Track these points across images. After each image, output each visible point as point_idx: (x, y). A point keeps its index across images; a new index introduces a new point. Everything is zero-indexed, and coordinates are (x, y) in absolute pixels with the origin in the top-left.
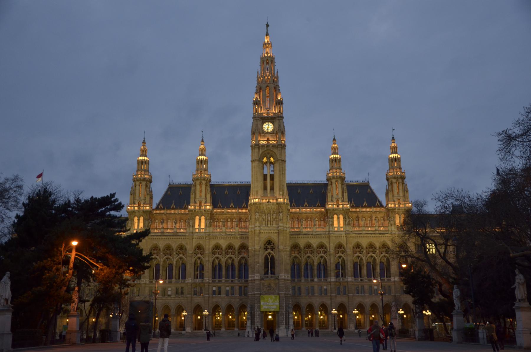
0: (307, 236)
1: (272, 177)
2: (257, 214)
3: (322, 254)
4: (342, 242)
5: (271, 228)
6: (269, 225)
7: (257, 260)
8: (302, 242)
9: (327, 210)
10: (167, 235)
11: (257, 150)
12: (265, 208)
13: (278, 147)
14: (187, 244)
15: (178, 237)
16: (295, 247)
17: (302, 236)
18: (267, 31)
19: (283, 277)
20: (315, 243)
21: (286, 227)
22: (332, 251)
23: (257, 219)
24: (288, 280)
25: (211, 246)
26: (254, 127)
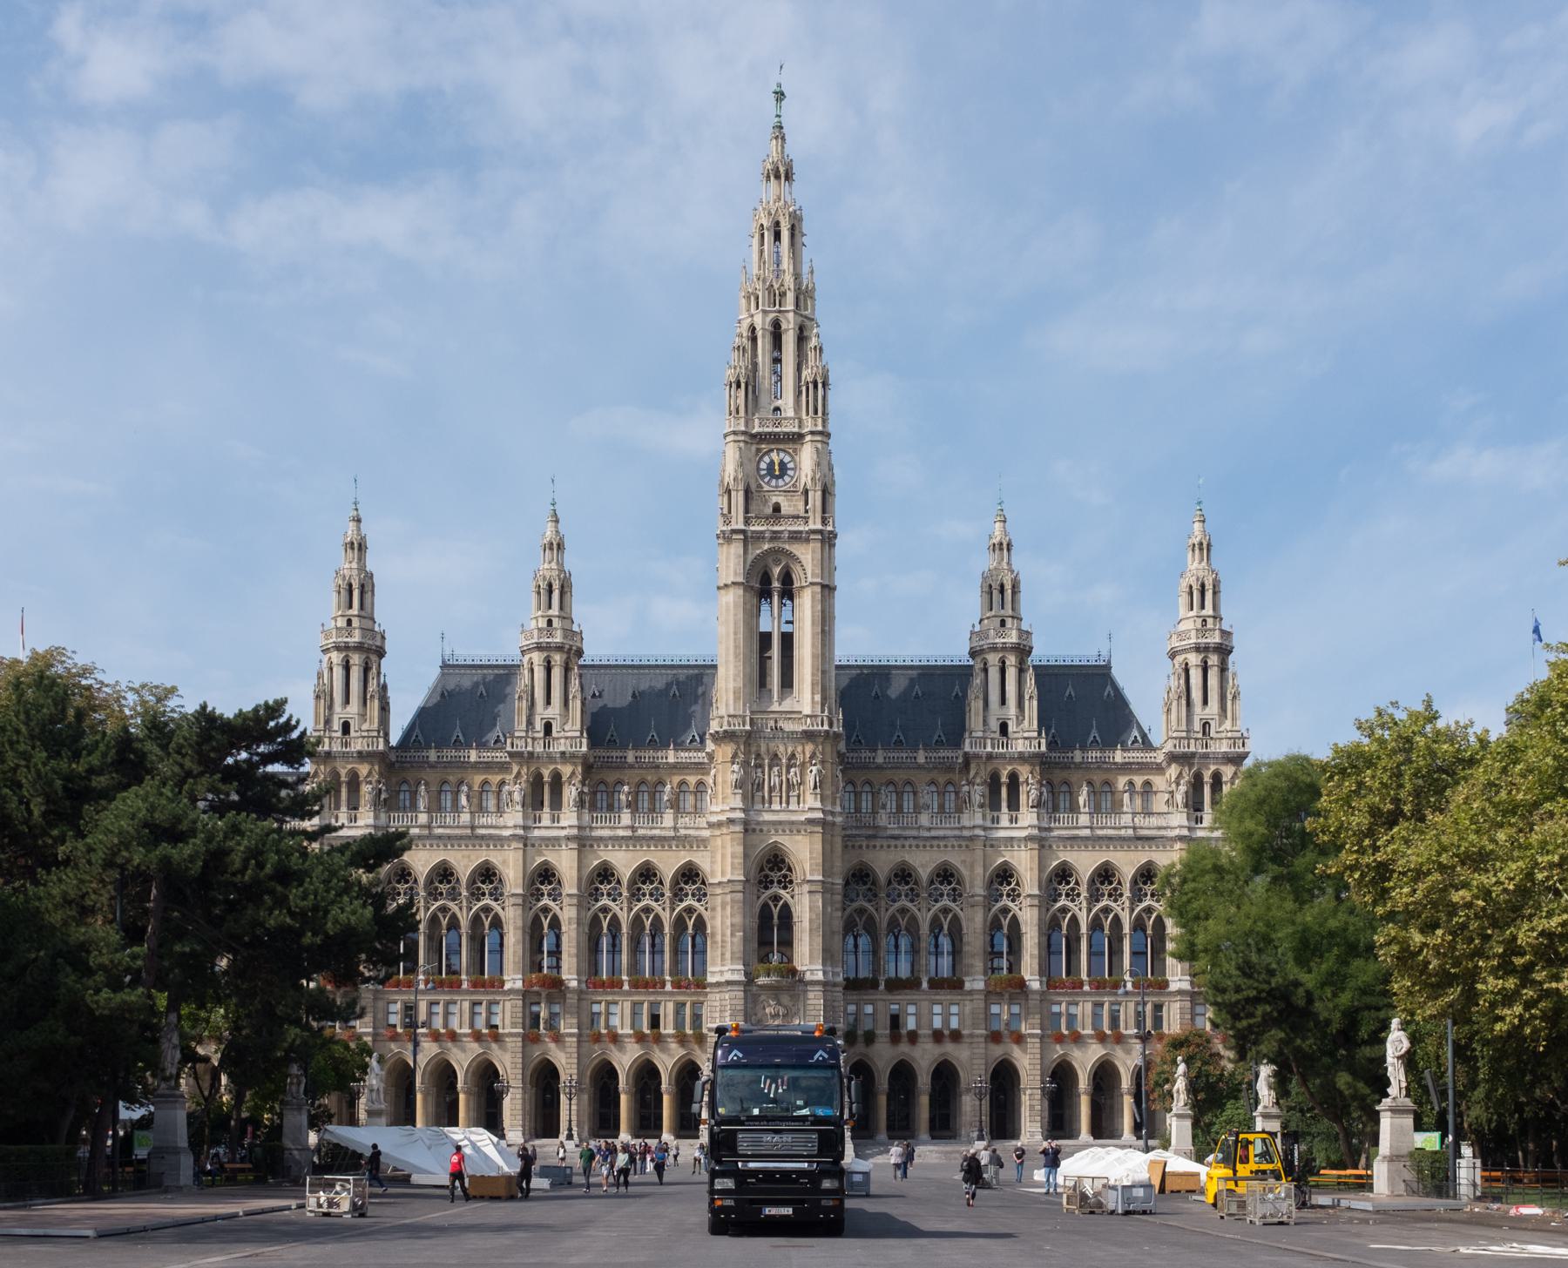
0: (899, 843)
1: (787, 640)
2: (736, 767)
3: (945, 902)
4: (1014, 862)
5: (783, 817)
9: (968, 759)
10: (440, 837)
12: (763, 749)
14: (504, 862)
16: (860, 877)
17: (885, 844)
19: (820, 976)
20: (924, 863)
21: (832, 813)
22: (980, 890)
24: (835, 985)
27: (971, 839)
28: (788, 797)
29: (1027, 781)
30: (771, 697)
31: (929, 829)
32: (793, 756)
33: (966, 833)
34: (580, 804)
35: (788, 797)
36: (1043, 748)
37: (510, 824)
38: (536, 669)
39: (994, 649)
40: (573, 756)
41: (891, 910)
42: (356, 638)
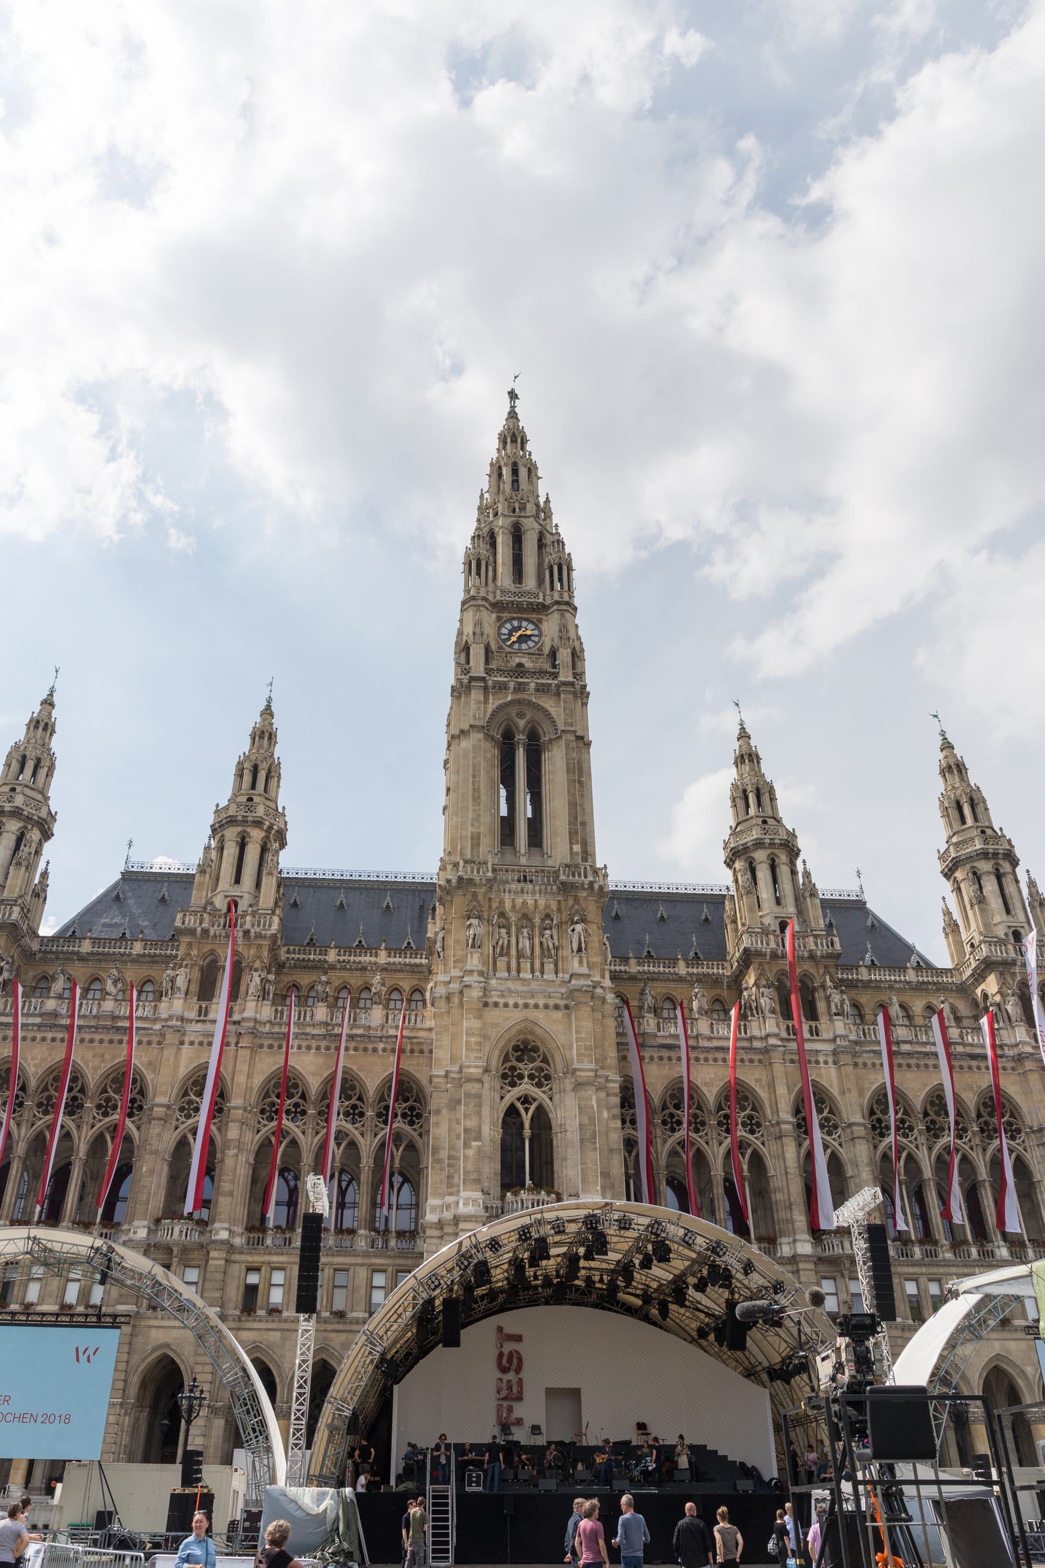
0: (673, 1054)
2: (474, 921)
5: (534, 986)
6: (526, 975)
7: (471, 1123)
8: (656, 1078)
11: (476, 695)
12: (508, 905)
13: (558, 694)
15: (116, 1037)
18: (513, 407)
20: (710, 1080)
22: (786, 1115)
23: (475, 944)
25: (258, 1080)
26: (469, 629)
27: (766, 1051)
28: (542, 965)
29: (823, 987)
30: (515, 852)
31: (710, 1039)
32: (548, 916)
33: (757, 1044)
34: (263, 995)
35: (542, 965)
36: (838, 946)
37: (164, 1016)
38: (227, 845)
39: (759, 844)
40: (259, 936)
41: (670, 1141)
42: (19, 801)
